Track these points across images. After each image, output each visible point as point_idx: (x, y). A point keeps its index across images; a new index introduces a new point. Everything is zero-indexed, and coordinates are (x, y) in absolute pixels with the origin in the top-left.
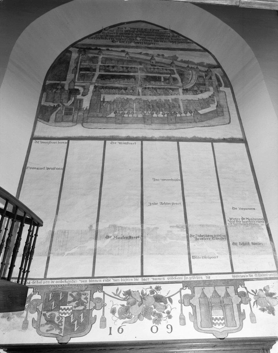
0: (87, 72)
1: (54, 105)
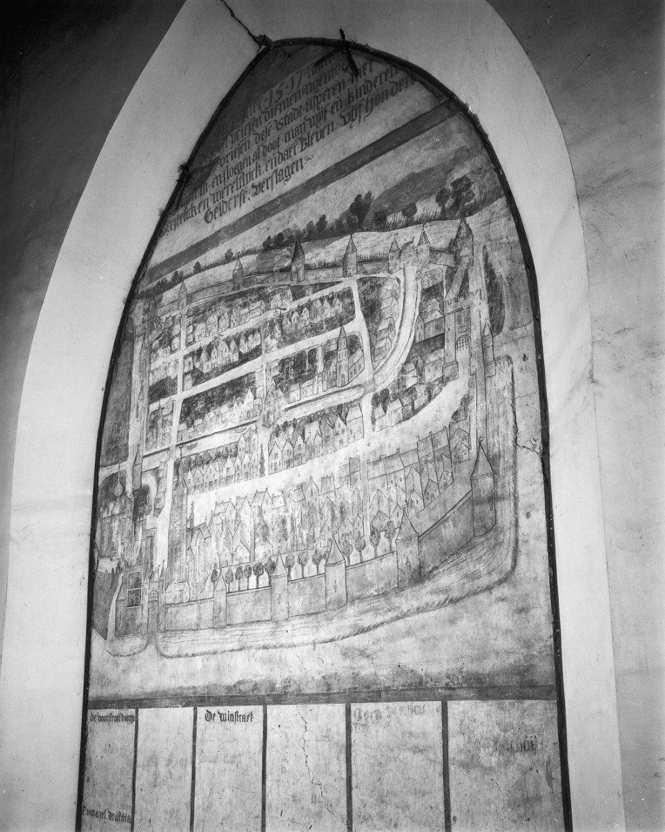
0: (163, 402)
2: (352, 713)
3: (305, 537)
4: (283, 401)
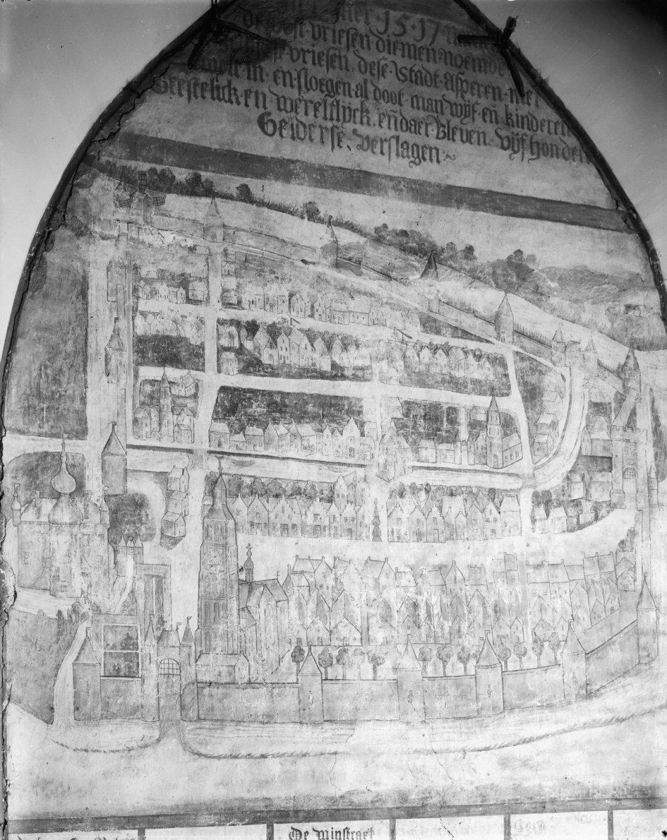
0: (172, 373)
1: (60, 613)
2: (512, 824)
3: (447, 630)
4: (410, 455)
